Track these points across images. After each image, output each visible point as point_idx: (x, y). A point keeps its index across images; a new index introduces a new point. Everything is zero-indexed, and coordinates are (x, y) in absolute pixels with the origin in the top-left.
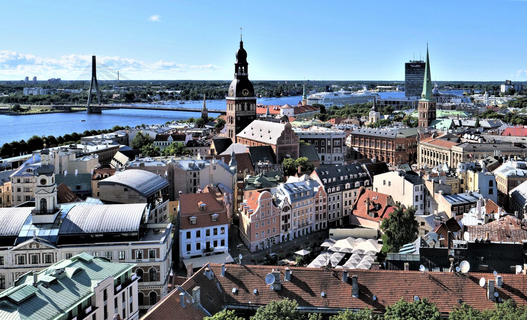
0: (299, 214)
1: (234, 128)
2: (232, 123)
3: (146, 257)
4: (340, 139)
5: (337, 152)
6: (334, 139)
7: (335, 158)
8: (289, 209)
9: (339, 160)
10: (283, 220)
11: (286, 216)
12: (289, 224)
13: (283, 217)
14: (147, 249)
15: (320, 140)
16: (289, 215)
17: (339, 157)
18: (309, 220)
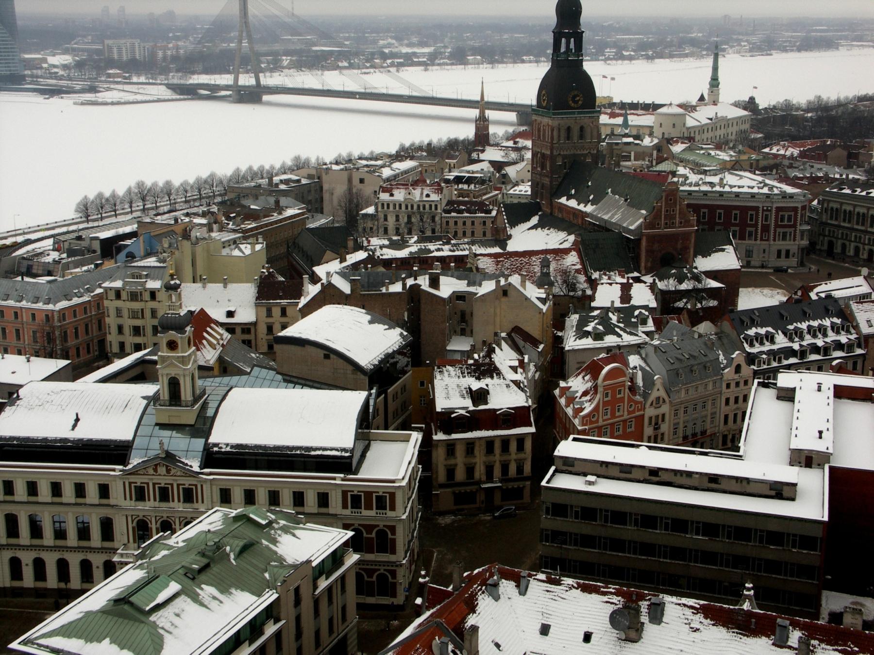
0: (685, 412)
1: (546, 181)
2: (542, 169)
3: (369, 507)
4: (795, 209)
5: (784, 239)
6: (779, 209)
7: (779, 253)
8: (664, 401)
9: (787, 256)
10: (650, 424)
11: (657, 417)
12: (663, 434)
13: (651, 418)
14: (372, 493)
15: (744, 210)
16: (663, 415)
17: (788, 252)
18: (708, 425)
